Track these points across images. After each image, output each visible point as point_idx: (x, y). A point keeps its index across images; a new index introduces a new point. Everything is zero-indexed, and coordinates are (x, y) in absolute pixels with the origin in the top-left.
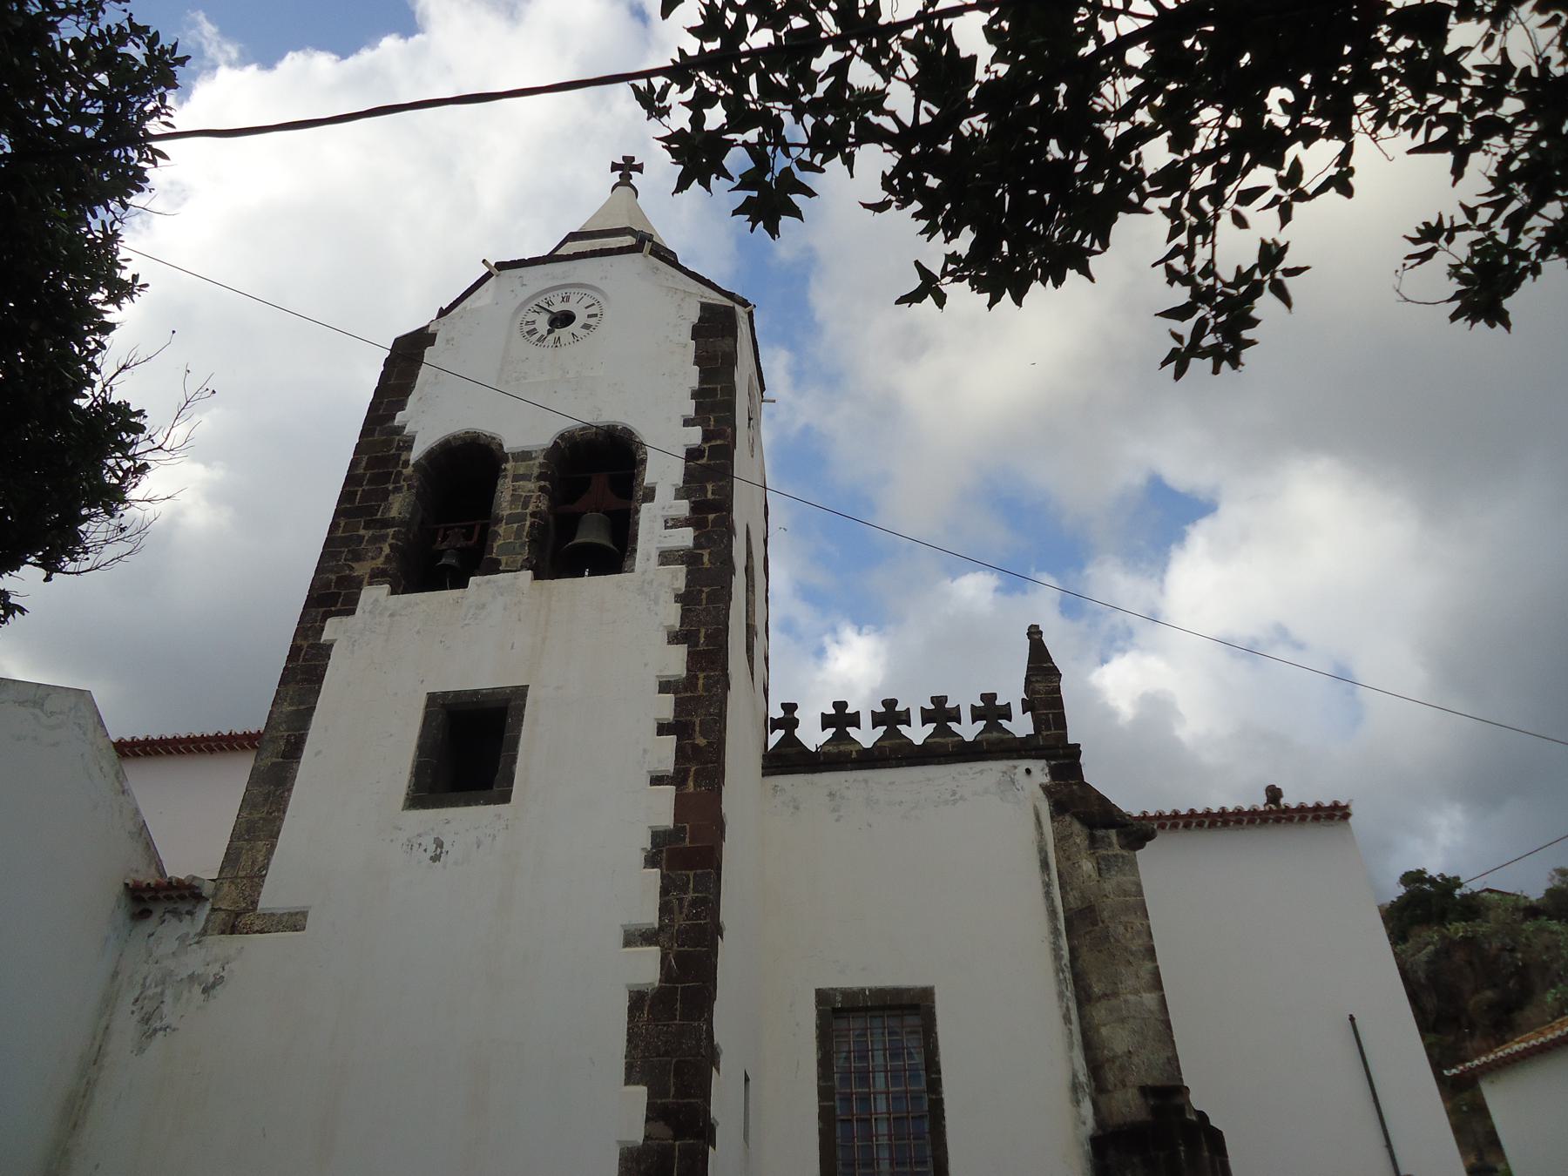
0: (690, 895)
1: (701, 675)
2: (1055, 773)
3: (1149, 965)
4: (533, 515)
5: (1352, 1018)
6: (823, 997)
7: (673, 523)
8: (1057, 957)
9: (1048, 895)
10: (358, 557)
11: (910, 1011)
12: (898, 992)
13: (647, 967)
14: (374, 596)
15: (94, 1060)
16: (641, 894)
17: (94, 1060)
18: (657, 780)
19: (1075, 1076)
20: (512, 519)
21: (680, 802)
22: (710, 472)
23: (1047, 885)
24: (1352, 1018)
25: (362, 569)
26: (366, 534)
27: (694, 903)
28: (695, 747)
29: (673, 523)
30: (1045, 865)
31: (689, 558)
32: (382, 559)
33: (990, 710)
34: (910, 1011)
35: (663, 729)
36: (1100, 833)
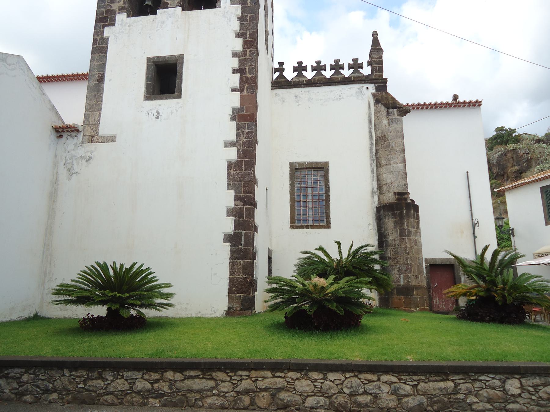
0: (246, 130)
1: (248, 50)
2: (377, 89)
3: (402, 155)
5: (467, 173)
6: (291, 164)
8: (371, 152)
11: (322, 169)
12: (317, 163)
13: (232, 154)
14: (121, 18)
15: (55, 182)
16: (230, 130)
17: (55, 182)
18: (233, 90)
19: (373, 189)
21: (242, 97)
24: (467, 173)
25: (115, 6)
27: (248, 133)
28: (247, 78)
30: (370, 122)
33: (356, 65)
34: (322, 169)
35: (235, 71)
36: (390, 110)
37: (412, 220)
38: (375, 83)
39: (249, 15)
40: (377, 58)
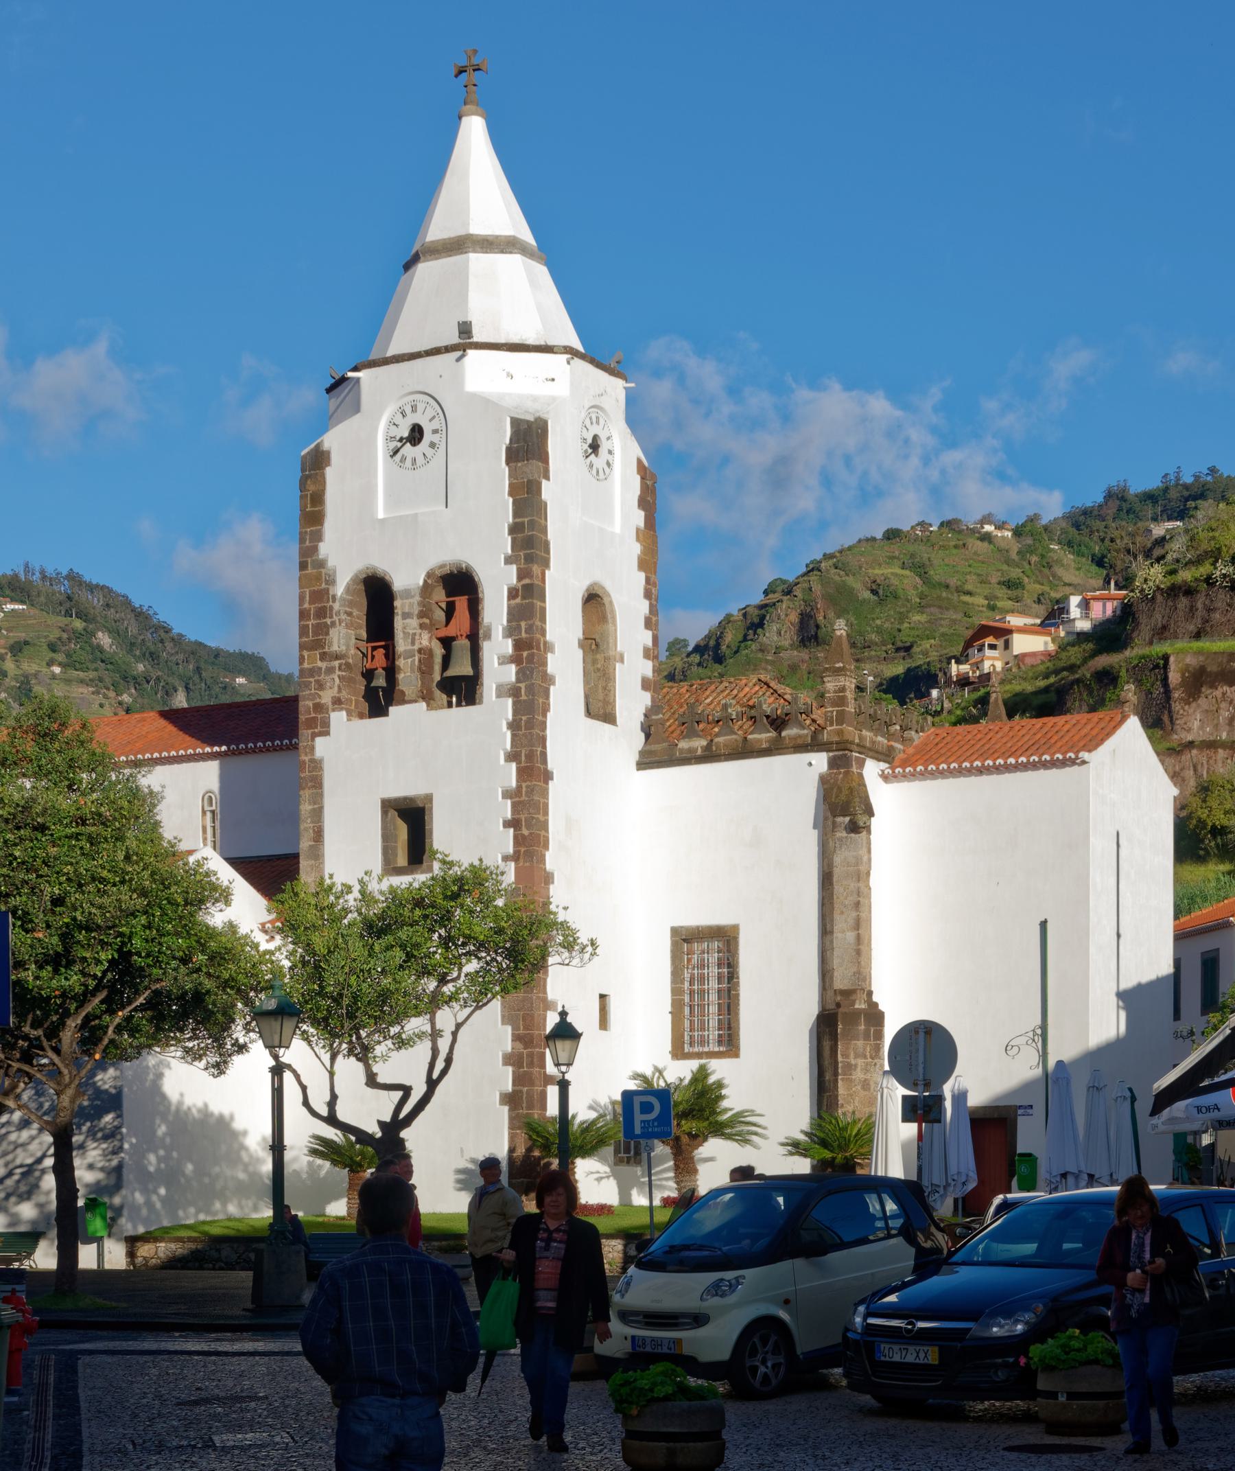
1: (524, 785)
2: (832, 763)
3: (854, 914)
4: (420, 651)
7: (504, 661)
10: (321, 686)
11: (724, 939)
20: (409, 654)
22: (528, 600)
25: (326, 697)
26: (323, 665)
28: (523, 835)
29: (504, 661)
31: (514, 692)
32: (336, 689)
34: (724, 939)
35: (507, 824)
37: (860, 1043)
38: (828, 751)
39: (524, 718)
40: (835, 692)
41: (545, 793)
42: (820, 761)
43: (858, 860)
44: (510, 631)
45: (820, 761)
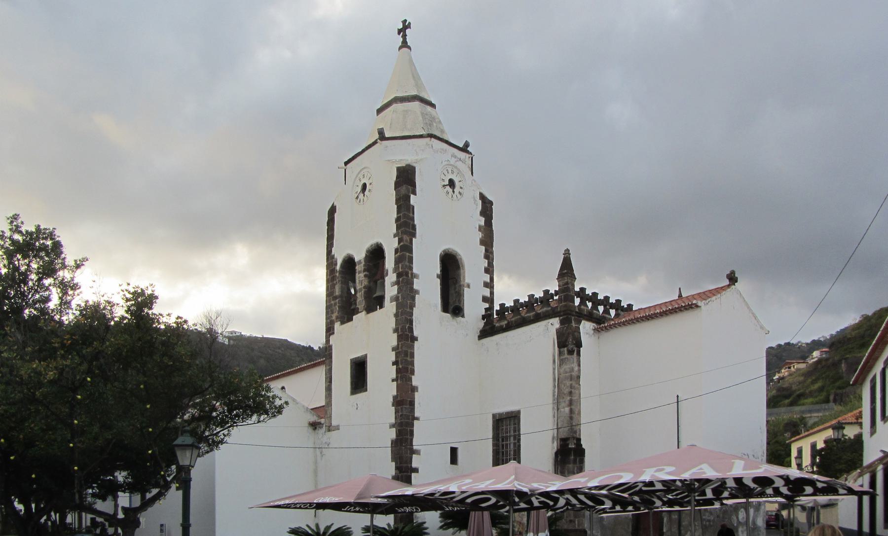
2: (562, 322)
7: (393, 284)
8: (554, 395)
9: (554, 373)
13: (393, 434)
15: (316, 462)
16: (389, 415)
17: (316, 462)
18: (393, 381)
23: (554, 369)
29: (393, 284)
30: (554, 361)
37: (571, 466)
38: (559, 316)
41: (412, 347)
42: (555, 323)
43: (572, 370)
44: (396, 269)
45: (555, 323)
